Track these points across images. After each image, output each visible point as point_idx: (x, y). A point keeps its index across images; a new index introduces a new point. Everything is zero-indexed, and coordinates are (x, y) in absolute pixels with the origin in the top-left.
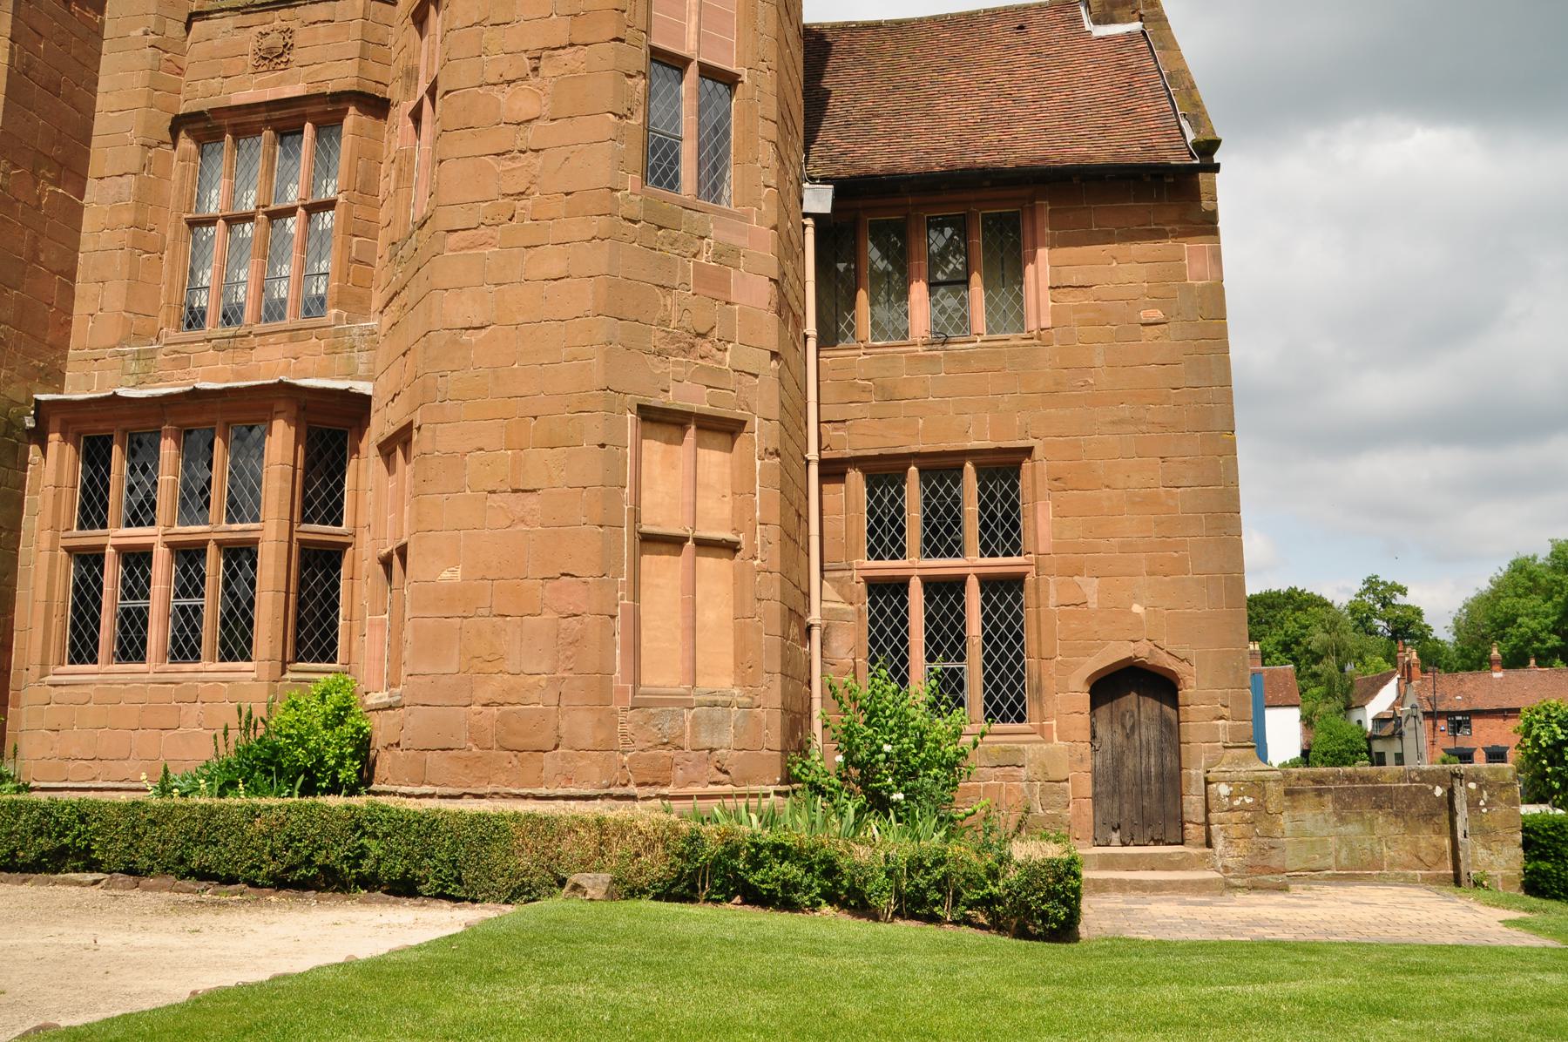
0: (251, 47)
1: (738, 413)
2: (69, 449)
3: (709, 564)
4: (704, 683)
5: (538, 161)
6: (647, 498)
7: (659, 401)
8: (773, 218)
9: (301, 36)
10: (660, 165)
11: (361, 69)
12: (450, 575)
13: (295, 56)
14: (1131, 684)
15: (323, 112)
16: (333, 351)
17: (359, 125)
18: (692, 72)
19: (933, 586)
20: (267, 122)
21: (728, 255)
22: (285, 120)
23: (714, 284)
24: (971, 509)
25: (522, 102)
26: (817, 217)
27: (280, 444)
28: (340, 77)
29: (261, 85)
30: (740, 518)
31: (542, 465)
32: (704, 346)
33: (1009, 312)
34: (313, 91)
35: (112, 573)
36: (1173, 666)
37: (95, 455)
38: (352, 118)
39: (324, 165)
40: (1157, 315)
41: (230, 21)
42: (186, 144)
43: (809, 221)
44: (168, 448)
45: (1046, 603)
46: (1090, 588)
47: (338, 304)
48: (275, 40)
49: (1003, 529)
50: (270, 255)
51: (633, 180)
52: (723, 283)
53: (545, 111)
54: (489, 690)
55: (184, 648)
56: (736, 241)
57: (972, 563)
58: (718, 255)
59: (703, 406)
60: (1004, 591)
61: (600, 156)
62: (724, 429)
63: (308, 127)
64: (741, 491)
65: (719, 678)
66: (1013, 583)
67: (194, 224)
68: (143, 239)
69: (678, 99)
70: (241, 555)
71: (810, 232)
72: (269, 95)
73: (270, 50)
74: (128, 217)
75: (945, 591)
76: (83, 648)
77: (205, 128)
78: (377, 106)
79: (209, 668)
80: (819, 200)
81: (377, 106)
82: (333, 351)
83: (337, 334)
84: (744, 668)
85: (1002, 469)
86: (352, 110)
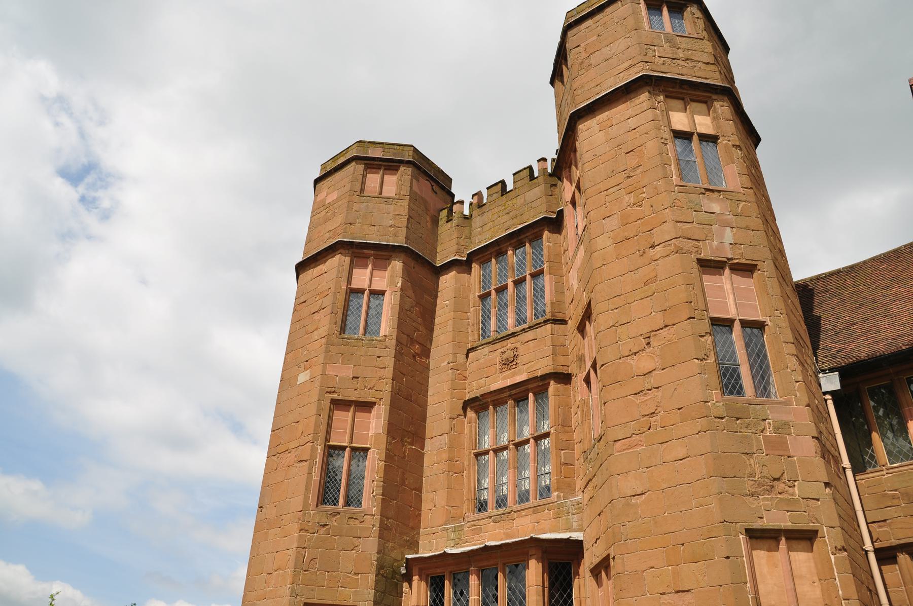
0: (498, 360)
1: (811, 526)
2: (423, 584)
5: (659, 393)
6: (761, 587)
7: (758, 525)
8: (805, 400)
9: (521, 351)
10: (730, 382)
11: (554, 360)
13: (519, 360)
15: (538, 386)
16: (557, 516)
17: (557, 390)
18: (737, 326)
20: (510, 396)
21: (782, 428)
22: (517, 394)
23: (778, 447)
25: (644, 363)
26: (833, 393)
27: (534, 574)
28: (544, 367)
29: (505, 378)
31: (690, 574)
32: (780, 486)
34: (531, 376)
37: (436, 586)
38: (553, 386)
39: (541, 414)
41: (486, 349)
42: (471, 414)
43: (828, 397)
44: (473, 580)
47: (558, 489)
48: (509, 354)
50: (518, 466)
51: (716, 394)
52: (783, 444)
53: (658, 365)
56: (785, 418)
58: (776, 429)
59: (787, 524)
61: (695, 384)
62: (804, 538)
63: (531, 395)
67: (477, 455)
68: (453, 467)
69: (732, 343)
71: (830, 403)
72: (509, 382)
73: (507, 360)
74: (445, 456)
77: (478, 405)
78: (565, 378)
80: (831, 382)
81: (565, 378)
82: (557, 516)
83: (560, 506)
86: (552, 382)
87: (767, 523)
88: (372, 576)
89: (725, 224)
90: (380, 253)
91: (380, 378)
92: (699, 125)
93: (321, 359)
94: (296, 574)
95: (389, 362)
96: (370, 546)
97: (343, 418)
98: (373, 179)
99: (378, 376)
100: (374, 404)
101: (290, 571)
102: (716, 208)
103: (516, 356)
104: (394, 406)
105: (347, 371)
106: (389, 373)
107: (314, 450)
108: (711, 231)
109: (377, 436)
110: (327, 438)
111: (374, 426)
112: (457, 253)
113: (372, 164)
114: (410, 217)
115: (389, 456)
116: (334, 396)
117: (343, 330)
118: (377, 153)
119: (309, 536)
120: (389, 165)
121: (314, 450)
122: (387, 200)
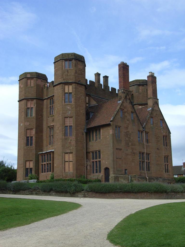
1: (72, 152)
3: (70, 163)
4: (70, 171)
6: (66, 159)
7: (66, 152)
12: (56, 165)
13: (54, 120)
14: (107, 169)
18: (68, 126)
19: (96, 161)
21: (71, 140)
23: (70, 143)
24: (98, 155)
26: (85, 132)
30: (73, 160)
33: (100, 138)
35: (44, 166)
36: (109, 167)
37: (48, 155)
40: (108, 137)
41: (50, 118)
42: (49, 129)
43: (85, 133)
45: (102, 163)
46: (104, 161)
49: (100, 158)
54: (57, 173)
55: (48, 172)
57: (98, 160)
60: (100, 161)
62: (72, 153)
64: (73, 157)
65: (71, 171)
66: (100, 161)
70: (50, 164)
71: (85, 133)
75: (96, 162)
76: (42, 172)
79: (49, 173)
84: (73, 170)
85: (99, 152)
87: (67, 152)
88: (35, 156)
89: (70, 110)
90: (32, 99)
91: (34, 124)
92: (70, 90)
93: (24, 121)
94: (24, 157)
95: (35, 121)
96: (34, 152)
97: (28, 131)
98: (29, 81)
99: (34, 124)
100: (33, 129)
101: (23, 156)
102: (69, 108)
103: (54, 120)
104: (36, 128)
105: (28, 124)
106: (35, 123)
107: (24, 138)
108: (67, 112)
109: (34, 134)
110: (26, 135)
111: (33, 132)
112: (47, 96)
113: (28, 78)
114: (37, 90)
115: (36, 137)
116: (27, 128)
117: (27, 116)
118: (29, 76)
119: (25, 151)
120: (31, 78)
121: (24, 138)
122: (32, 87)
